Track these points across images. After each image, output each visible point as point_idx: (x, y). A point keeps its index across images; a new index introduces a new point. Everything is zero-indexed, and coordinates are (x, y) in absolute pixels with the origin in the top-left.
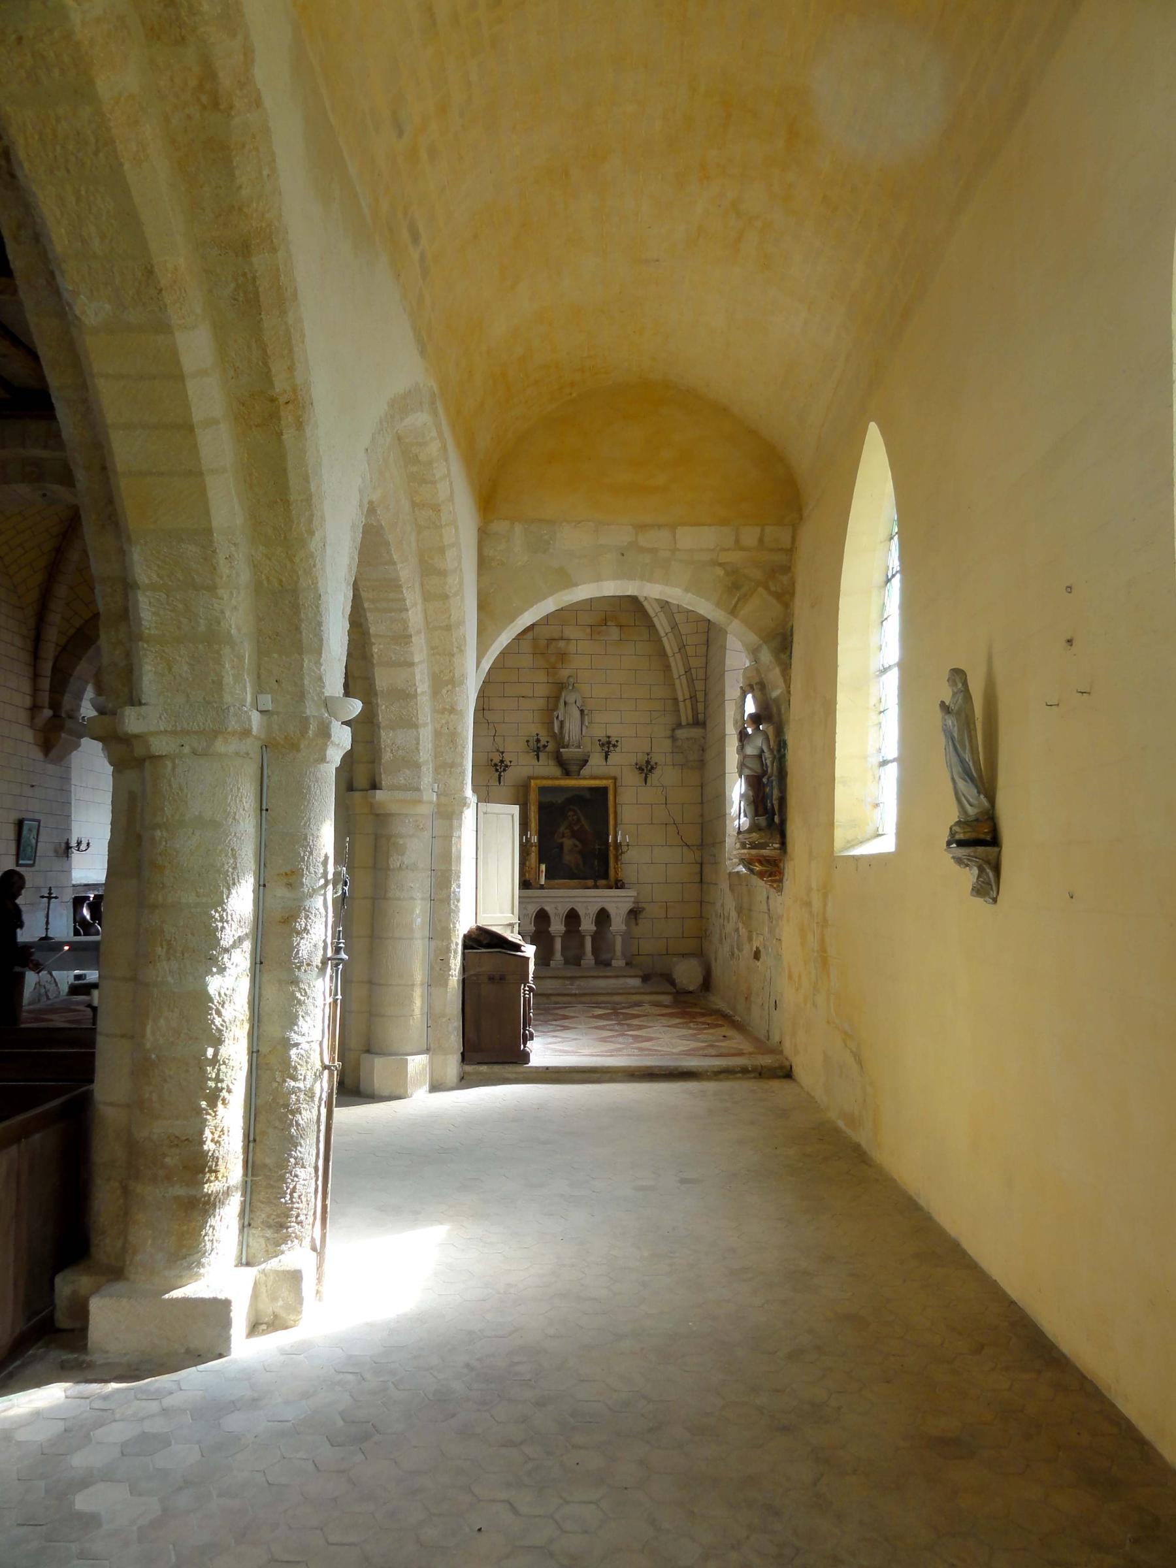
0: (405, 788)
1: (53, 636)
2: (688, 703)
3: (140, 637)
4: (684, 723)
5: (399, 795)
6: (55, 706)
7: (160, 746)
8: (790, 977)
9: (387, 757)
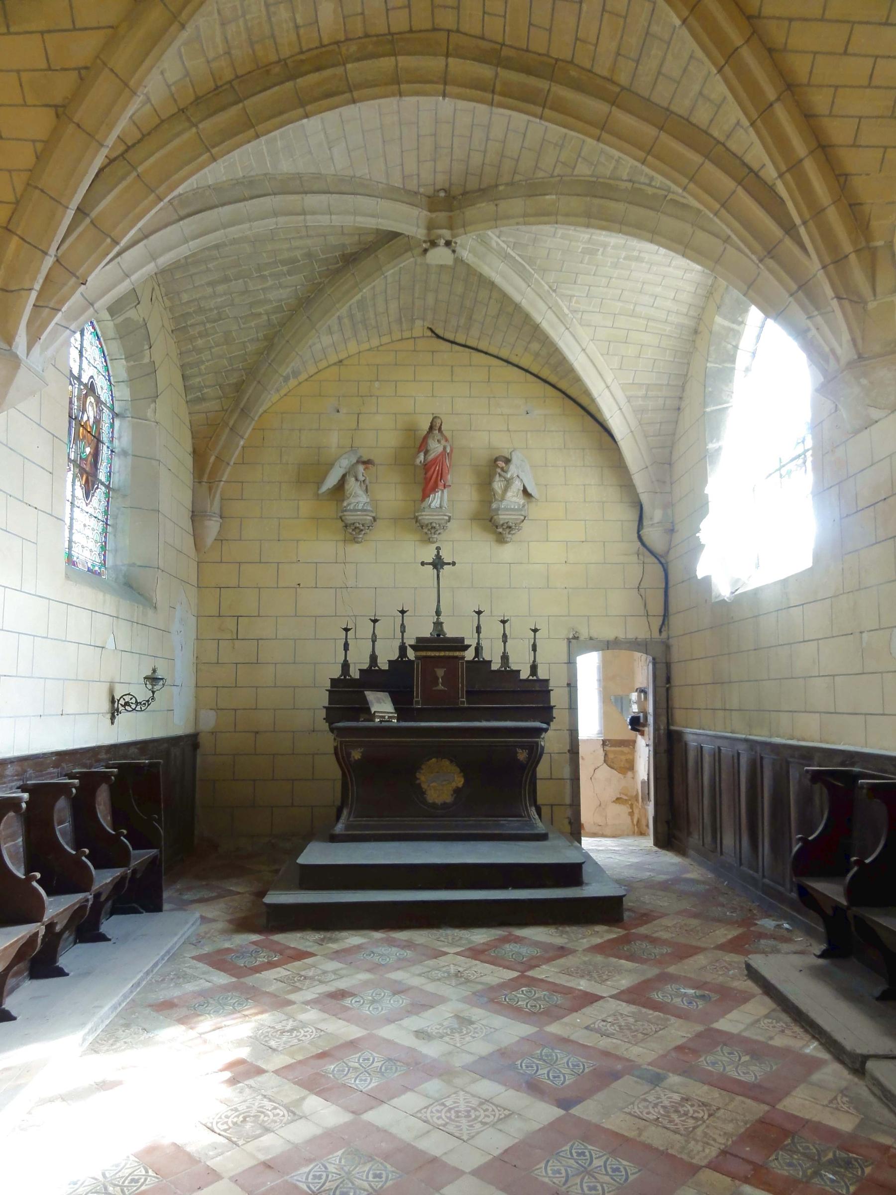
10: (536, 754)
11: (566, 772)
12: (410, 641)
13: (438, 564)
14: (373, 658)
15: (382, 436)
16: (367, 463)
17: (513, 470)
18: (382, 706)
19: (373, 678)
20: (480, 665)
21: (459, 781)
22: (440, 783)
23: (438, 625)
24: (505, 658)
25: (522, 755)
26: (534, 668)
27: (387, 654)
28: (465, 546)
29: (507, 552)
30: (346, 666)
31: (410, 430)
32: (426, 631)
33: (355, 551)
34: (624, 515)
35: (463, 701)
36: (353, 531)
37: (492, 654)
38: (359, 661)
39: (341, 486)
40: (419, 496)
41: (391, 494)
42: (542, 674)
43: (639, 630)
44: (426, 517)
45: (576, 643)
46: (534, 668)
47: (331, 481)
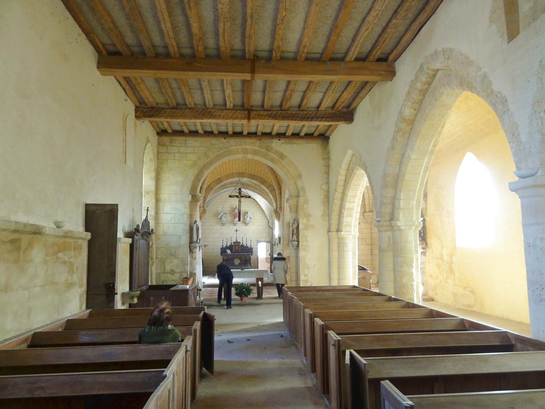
1: (205, 187)
3: (400, 208)
5: (347, 233)
6: (203, 206)
7: (402, 228)
8: (431, 276)
9: (344, 224)
10: (250, 258)
13: (236, 231)
15: (227, 208)
18: (229, 251)
19: (227, 248)
20: (243, 246)
21: (239, 261)
22: (237, 262)
27: (229, 244)
28: (240, 226)
29: (247, 227)
31: (232, 207)
32: (235, 241)
34: (266, 221)
36: (223, 224)
37: (245, 244)
38: (225, 245)
43: (268, 239)
44: (235, 222)
45: (258, 242)
47: (220, 216)
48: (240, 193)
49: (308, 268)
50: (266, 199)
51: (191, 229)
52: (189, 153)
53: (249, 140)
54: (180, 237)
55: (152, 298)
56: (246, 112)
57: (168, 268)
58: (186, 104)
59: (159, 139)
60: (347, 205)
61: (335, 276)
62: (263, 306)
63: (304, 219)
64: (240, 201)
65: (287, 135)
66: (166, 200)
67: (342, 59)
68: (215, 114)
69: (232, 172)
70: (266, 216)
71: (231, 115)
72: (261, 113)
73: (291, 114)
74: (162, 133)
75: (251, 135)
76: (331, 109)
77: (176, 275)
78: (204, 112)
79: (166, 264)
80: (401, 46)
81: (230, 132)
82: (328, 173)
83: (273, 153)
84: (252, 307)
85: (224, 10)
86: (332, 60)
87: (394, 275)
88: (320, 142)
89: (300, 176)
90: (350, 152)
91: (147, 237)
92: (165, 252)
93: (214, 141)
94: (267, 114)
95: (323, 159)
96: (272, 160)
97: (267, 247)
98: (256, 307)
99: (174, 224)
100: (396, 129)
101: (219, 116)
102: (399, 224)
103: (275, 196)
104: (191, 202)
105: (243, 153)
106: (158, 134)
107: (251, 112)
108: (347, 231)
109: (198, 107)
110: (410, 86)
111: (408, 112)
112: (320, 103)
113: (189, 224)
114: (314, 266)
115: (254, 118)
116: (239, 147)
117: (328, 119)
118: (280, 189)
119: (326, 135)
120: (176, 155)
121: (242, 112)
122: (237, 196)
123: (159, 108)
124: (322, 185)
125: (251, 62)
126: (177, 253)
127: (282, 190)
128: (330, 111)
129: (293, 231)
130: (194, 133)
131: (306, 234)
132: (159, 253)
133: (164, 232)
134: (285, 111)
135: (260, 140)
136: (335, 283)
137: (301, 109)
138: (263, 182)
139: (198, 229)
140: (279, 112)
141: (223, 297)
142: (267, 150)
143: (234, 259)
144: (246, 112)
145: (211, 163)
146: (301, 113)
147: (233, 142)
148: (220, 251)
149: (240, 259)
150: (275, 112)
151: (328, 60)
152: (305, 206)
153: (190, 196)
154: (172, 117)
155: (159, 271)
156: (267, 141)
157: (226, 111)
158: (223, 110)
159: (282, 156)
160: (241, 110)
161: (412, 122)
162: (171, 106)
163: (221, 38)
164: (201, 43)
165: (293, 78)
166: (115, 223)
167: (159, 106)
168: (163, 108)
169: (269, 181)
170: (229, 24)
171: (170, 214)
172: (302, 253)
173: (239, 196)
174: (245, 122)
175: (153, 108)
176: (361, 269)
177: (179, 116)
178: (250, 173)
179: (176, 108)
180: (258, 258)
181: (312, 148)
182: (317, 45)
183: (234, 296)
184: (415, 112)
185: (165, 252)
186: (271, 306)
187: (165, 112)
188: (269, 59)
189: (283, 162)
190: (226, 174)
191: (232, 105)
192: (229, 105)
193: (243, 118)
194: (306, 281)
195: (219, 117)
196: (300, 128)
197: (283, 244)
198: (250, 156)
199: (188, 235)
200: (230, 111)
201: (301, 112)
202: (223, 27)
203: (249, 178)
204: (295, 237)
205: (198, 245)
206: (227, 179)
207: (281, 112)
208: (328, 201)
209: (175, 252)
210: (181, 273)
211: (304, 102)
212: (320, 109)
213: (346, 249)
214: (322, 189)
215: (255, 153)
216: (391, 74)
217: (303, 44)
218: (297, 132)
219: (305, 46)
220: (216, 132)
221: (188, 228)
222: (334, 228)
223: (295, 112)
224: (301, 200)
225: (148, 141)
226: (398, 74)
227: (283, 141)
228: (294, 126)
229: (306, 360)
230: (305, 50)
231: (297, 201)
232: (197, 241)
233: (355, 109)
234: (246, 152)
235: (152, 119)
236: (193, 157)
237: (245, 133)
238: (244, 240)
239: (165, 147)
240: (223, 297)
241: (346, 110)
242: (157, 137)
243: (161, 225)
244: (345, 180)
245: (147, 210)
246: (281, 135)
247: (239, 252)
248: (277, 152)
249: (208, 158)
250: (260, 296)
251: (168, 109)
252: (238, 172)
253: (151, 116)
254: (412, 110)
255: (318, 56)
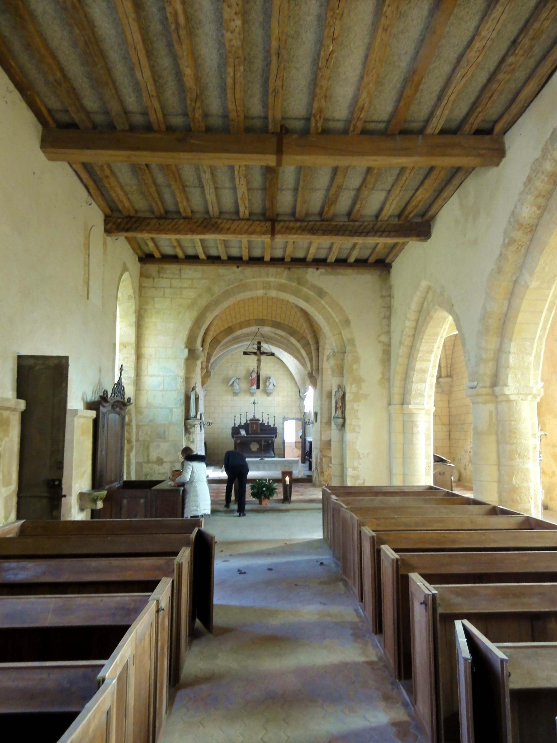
0: (419, 404)
1: (209, 339)
2: (445, 368)
3: (508, 367)
4: (443, 375)
5: (417, 407)
6: (207, 367)
7: (512, 398)
9: (413, 393)
11: (282, 447)
12: (248, 419)
13: (254, 403)
14: (240, 423)
15: (241, 371)
16: (239, 379)
17: (271, 380)
18: (243, 432)
19: (240, 427)
20: (263, 424)
22: (254, 447)
23: (254, 416)
24: (268, 422)
25: (270, 442)
26: (274, 425)
27: (243, 422)
29: (270, 398)
30: (235, 424)
31: (248, 370)
32: (252, 417)
33: (236, 398)
35: (259, 431)
36: (236, 394)
39: (232, 385)
40: (250, 385)
41: (244, 385)
42: (276, 426)
43: (299, 416)
44: (251, 391)
45: (285, 419)
46: (274, 425)
48: (259, 348)
49: (359, 457)
50: (297, 358)
51: (187, 399)
52: (186, 288)
53: (272, 270)
54: (171, 410)
55: (125, 501)
56: (269, 224)
57: (154, 455)
58: (179, 213)
59: (141, 268)
60: (418, 365)
61: (397, 469)
62: (291, 513)
63: (353, 386)
64: (259, 361)
65: (328, 261)
66: (151, 356)
67: (421, 131)
68: (222, 225)
69: (247, 319)
70: (296, 383)
71: (246, 228)
72: (292, 224)
73: (336, 225)
74: (146, 258)
75: (276, 261)
76: (397, 219)
77: (165, 465)
78: (207, 223)
79: (151, 449)
80: (516, 107)
81: (245, 257)
82: (388, 318)
83: (308, 288)
84: (274, 515)
85: (234, 42)
86: (404, 132)
87: (499, 470)
88: (378, 272)
89: (347, 322)
90: (424, 284)
91: (121, 409)
92: (149, 433)
93: (222, 270)
94: (300, 227)
95: (383, 297)
96: (307, 299)
97: (297, 426)
98: (282, 514)
99: (163, 391)
100: (506, 241)
101: (229, 229)
102: (507, 392)
103: (309, 354)
104: (187, 359)
105: (264, 288)
106: (141, 260)
107: (276, 223)
108: (416, 404)
109: (197, 215)
110: (532, 169)
111: (527, 212)
112: (381, 209)
113: (183, 391)
114: (368, 454)
115: (280, 232)
116: (258, 279)
117: (393, 234)
118: (317, 343)
119: (388, 261)
120: (167, 291)
121: (263, 224)
122: (255, 353)
123: (139, 218)
124: (380, 335)
125: (277, 137)
126: (167, 433)
127: (321, 344)
128: (395, 221)
129: (336, 403)
130: (192, 259)
131: (356, 407)
132: (140, 433)
133: (148, 402)
134: (327, 221)
135: (289, 269)
136: (397, 482)
137: (352, 217)
138: (293, 332)
139: (197, 399)
140: (319, 223)
141: (233, 498)
142: (299, 283)
143: (250, 444)
144: (269, 224)
145: (216, 303)
146: (352, 225)
147: (249, 273)
148: (230, 431)
149: (259, 442)
150: (311, 224)
151: (398, 133)
152: (355, 367)
153: (186, 351)
154: (159, 231)
155: (141, 460)
156: (299, 271)
157: (239, 222)
158: (233, 220)
159: (321, 293)
160: (261, 221)
161: (532, 229)
162: (157, 214)
163: (230, 96)
164: (198, 104)
165: (343, 161)
166: (64, 385)
167: (139, 215)
168: (145, 219)
169: (302, 332)
170: (242, 68)
171: (158, 376)
172: (349, 436)
173: (258, 353)
174: (267, 238)
175: (131, 217)
176: (438, 460)
177: (169, 230)
178: (274, 319)
179: (165, 218)
180: (284, 443)
181: (366, 280)
182: (382, 109)
183: (249, 497)
184: (538, 212)
185: (149, 433)
186: (304, 513)
187: (149, 223)
188: (305, 132)
189: (323, 302)
190: (239, 321)
191: (247, 212)
192: (243, 211)
193: (265, 233)
194: (356, 478)
195: (228, 231)
196: (348, 251)
197: (321, 423)
198: (273, 293)
199: (183, 408)
200: (243, 223)
201: (351, 223)
202: (232, 74)
203: (272, 326)
204: (339, 412)
205: (197, 422)
206: (241, 328)
207: (323, 223)
208: (389, 360)
209: (164, 432)
210: (172, 462)
211: (357, 206)
212: (380, 218)
213: (415, 430)
214: (379, 342)
215: (281, 288)
216: (498, 153)
217: (360, 103)
218: (343, 256)
219: (362, 108)
220: (224, 257)
221: (182, 397)
222: (396, 399)
223: (341, 224)
224: (349, 358)
225: (125, 269)
226: (509, 154)
227: (322, 270)
228: (341, 245)
229: (364, 610)
230: (363, 115)
231: (343, 360)
232: (196, 417)
233: (433, 217)
234: (267, 286)
235: (130, 234)
236: (191, 294)
237: (267, 258)
238: (265, 417)
239: (150, 280)
240: (233, 498)
241: (419, 220)
242: (139, 265)
243: (144, 392)
244: (416, 328)
245: (121, 369)
246: (319, 262)
247: (258, 434)
248: (313, 287)
249: (212, 295)
250: (287, 499)
251: (152, 219)
252: (256, 317)
253: (127, 230)
254: (535, 208)
255: (382, 126)
